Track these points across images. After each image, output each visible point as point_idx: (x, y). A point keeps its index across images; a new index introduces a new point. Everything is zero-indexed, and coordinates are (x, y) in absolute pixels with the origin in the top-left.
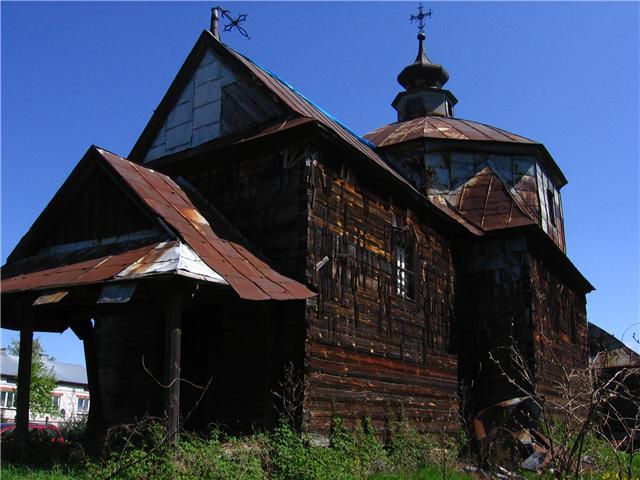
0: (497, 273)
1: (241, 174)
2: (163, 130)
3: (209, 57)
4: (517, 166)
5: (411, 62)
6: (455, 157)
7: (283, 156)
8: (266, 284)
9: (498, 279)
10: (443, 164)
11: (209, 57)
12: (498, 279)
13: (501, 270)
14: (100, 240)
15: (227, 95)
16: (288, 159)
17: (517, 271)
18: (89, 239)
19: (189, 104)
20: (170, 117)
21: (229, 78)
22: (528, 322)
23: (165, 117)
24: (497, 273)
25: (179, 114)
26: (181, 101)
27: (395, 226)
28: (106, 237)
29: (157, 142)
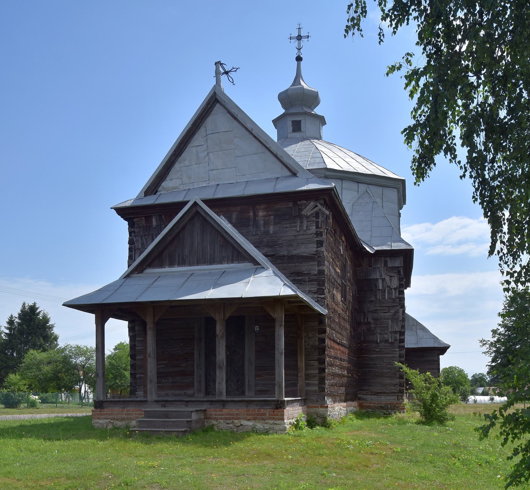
0: (380, 281)
5: (286, 84)
9: (381, 288)
12: (381, 288)
24: (380, 281)
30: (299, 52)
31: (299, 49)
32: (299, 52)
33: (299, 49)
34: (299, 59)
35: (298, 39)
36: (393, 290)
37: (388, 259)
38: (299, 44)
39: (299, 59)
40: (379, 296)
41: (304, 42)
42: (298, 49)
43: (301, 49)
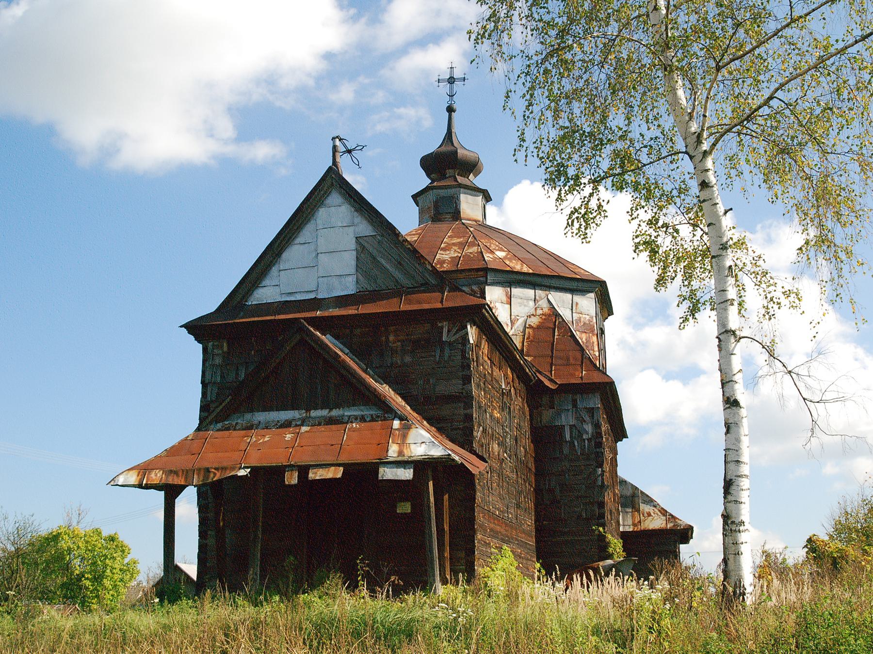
1: (391, 338)
2: (274, 270)
3: (335, 198)
4: (577, 304)
5: (433, 145)
6: (516, 291)
7: (442, 328)
8: (459, 455)
9: (568, 437)
10: (504, 299)
11: (335, 198)
12: (568, 437)
13: (571, 427)
14: (331, 410)
15: (363, 247)
16: (448, 331)
17: (589, 428)
18: (293, 408)
19: (312, 247)
20: (285, 255)
21: (365, 228)
22: (600, 483)
23: (279, 255)
25: (294, 254)
26: (298, 240)
27: (503, 387)
28: (316, 409)
29: (266, 282)
30: (451, 100)
31: (451, 96)
32: (451, 100)
33: (451, 96)
34: (450, 110)
35: (449, 83)
36: (586, 442)
37: (578, 397)
38: (451, 89)
39: (450, 110)
40: (566, 451)
41: (458, 85)
42: (449, 96)
43: (453, 95)
